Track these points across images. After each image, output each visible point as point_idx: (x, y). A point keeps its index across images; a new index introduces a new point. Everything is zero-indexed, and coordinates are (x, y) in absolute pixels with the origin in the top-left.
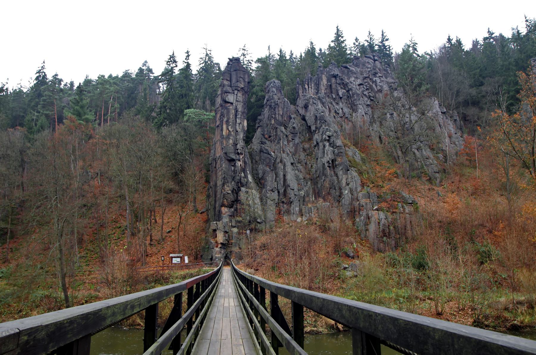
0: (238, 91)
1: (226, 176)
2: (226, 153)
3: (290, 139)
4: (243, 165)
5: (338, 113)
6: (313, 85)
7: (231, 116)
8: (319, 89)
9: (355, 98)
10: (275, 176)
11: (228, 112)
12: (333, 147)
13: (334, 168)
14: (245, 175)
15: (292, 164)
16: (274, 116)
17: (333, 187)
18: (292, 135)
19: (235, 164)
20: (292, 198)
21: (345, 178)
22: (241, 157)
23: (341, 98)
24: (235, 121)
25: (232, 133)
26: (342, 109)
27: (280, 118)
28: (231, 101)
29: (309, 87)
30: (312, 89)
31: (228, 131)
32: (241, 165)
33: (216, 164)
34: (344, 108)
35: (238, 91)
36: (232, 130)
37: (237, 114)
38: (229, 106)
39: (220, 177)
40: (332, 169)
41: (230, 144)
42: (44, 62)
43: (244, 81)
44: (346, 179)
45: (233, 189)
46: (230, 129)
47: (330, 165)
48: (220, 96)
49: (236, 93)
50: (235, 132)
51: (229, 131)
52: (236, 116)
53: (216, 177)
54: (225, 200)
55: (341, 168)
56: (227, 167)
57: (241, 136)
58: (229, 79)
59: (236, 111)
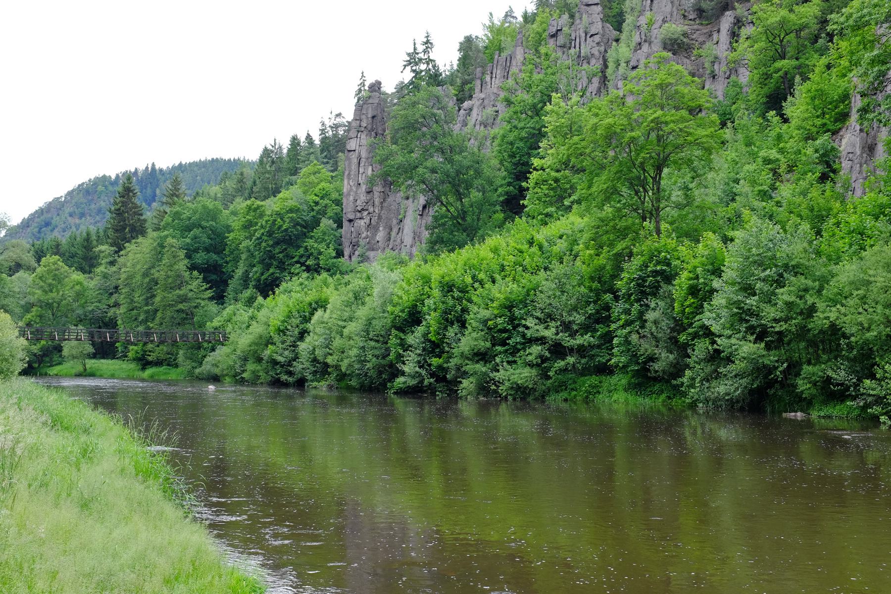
6: (499, 72)
22: (365, 213)
25: (353, 188)
29: (492, 78)
42: (363, 76)
46: (351, 183)
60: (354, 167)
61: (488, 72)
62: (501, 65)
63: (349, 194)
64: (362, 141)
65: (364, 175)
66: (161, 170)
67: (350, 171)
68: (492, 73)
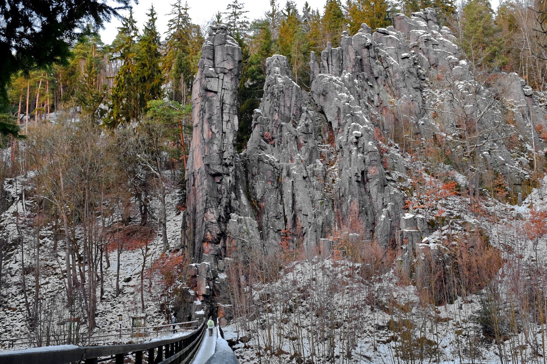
0: (225, 73)
1: (209, 198)
2: (208, 165)
3: (302, 142)
4: (233, 181)
5: (373, 101)
6: (334, 61)
7: (215, 112)
8: (344, 66)
9: (398, 78)
10: (280, 196)
11: (211, 106)
12: (363, 153)
13: (364, 184)
14: (236, 195)
15: (304, 178)
16: (277, 109)
17: (364, 212)
18: (304, 135)
19: (221, 180)
20: (305, 228)
22: (231, 169)
23: (376, 78)
24: (221, 118)
25: (217, 135)
26: (378, 94)
27: (287, 112)
29: (328, 64)
30: (334, 68)
31: (211, 133)
32: (230, 181)
33: (194, 181)
34: (381, 93)
35: (225, 73)
36: (217, 130)
37: (224, 108)
38: (212, 97)
39: (201, 200)
40: (362, 185)
41: (213, 152)
43: (234, 60)
44: (383, 199)
45: (220, 216)
46: (214, 130)
47: (360, 179)
48: (198, 83)
49: (221, 78)
50: (221, 133)
51: (213, 133)
52: (222, 110)
53: (195, 199)
54: (208, 233)
55: (375, 183)
56: (211, 185)
57: (231, 138)
58: (211, 57)
59: (223, 103)
61: (325, 58)
62: (336, 55)
64: (225, 84)
65: (229, 124)
68: (327, 60)
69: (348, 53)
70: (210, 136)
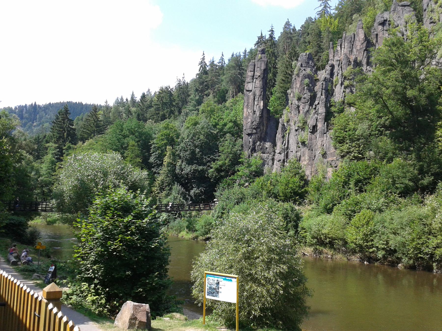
6: (346, 44)
21: (321, 141)
24: (253, 104)
25: (251, 114)
28: (250, 89)
30: (345, 49)
31: (248, 113)
42: (204, 54)
44: (322, 142)
50: (253, 112)
52: (254, 99)
60: (251, 101)
61: (339, 44)
63: (247, 118)
65: (258, 106)
66: (39, 106)
67: (248, 103)
68: (341, 45)
69: (358, 35)
70: (247, 115)
